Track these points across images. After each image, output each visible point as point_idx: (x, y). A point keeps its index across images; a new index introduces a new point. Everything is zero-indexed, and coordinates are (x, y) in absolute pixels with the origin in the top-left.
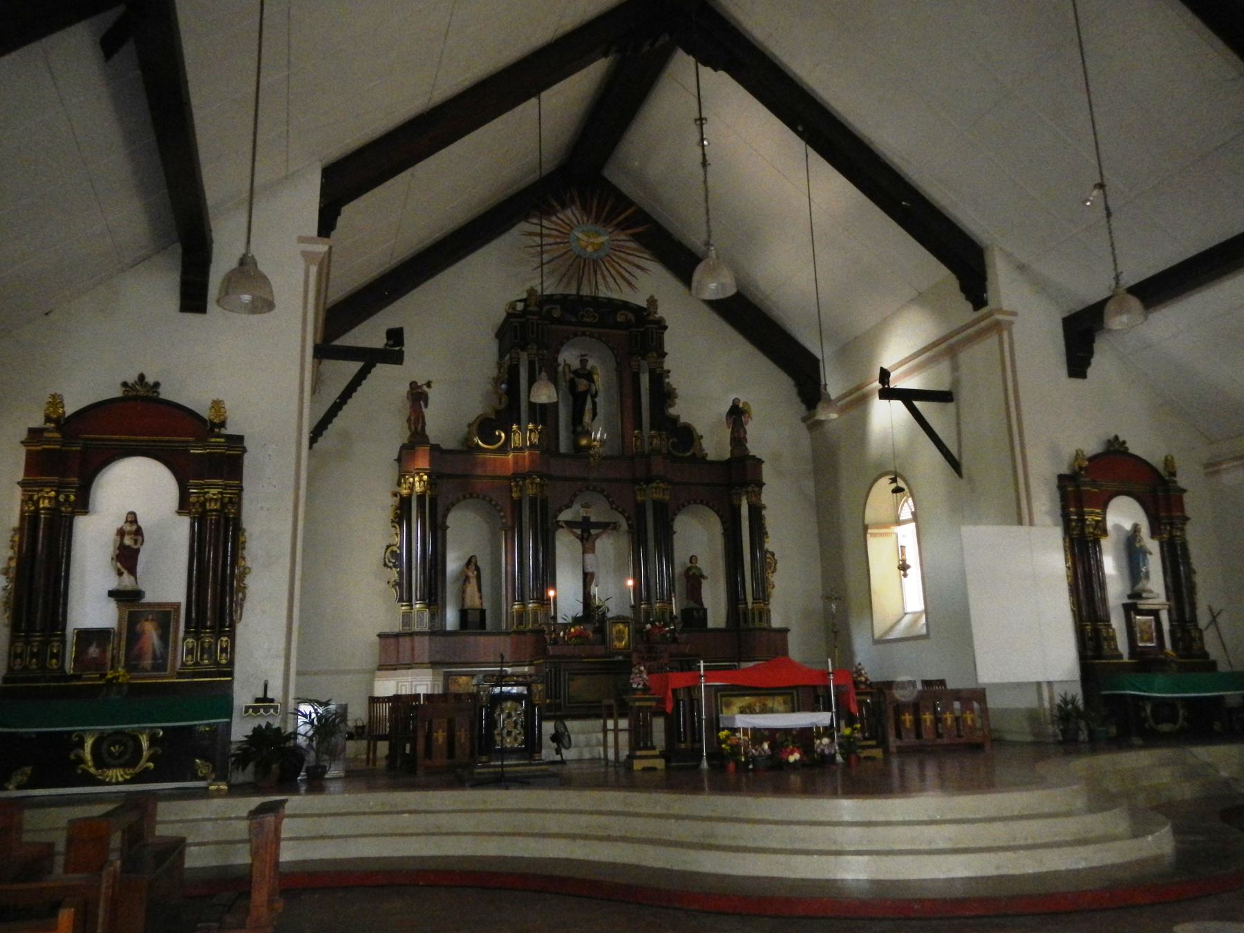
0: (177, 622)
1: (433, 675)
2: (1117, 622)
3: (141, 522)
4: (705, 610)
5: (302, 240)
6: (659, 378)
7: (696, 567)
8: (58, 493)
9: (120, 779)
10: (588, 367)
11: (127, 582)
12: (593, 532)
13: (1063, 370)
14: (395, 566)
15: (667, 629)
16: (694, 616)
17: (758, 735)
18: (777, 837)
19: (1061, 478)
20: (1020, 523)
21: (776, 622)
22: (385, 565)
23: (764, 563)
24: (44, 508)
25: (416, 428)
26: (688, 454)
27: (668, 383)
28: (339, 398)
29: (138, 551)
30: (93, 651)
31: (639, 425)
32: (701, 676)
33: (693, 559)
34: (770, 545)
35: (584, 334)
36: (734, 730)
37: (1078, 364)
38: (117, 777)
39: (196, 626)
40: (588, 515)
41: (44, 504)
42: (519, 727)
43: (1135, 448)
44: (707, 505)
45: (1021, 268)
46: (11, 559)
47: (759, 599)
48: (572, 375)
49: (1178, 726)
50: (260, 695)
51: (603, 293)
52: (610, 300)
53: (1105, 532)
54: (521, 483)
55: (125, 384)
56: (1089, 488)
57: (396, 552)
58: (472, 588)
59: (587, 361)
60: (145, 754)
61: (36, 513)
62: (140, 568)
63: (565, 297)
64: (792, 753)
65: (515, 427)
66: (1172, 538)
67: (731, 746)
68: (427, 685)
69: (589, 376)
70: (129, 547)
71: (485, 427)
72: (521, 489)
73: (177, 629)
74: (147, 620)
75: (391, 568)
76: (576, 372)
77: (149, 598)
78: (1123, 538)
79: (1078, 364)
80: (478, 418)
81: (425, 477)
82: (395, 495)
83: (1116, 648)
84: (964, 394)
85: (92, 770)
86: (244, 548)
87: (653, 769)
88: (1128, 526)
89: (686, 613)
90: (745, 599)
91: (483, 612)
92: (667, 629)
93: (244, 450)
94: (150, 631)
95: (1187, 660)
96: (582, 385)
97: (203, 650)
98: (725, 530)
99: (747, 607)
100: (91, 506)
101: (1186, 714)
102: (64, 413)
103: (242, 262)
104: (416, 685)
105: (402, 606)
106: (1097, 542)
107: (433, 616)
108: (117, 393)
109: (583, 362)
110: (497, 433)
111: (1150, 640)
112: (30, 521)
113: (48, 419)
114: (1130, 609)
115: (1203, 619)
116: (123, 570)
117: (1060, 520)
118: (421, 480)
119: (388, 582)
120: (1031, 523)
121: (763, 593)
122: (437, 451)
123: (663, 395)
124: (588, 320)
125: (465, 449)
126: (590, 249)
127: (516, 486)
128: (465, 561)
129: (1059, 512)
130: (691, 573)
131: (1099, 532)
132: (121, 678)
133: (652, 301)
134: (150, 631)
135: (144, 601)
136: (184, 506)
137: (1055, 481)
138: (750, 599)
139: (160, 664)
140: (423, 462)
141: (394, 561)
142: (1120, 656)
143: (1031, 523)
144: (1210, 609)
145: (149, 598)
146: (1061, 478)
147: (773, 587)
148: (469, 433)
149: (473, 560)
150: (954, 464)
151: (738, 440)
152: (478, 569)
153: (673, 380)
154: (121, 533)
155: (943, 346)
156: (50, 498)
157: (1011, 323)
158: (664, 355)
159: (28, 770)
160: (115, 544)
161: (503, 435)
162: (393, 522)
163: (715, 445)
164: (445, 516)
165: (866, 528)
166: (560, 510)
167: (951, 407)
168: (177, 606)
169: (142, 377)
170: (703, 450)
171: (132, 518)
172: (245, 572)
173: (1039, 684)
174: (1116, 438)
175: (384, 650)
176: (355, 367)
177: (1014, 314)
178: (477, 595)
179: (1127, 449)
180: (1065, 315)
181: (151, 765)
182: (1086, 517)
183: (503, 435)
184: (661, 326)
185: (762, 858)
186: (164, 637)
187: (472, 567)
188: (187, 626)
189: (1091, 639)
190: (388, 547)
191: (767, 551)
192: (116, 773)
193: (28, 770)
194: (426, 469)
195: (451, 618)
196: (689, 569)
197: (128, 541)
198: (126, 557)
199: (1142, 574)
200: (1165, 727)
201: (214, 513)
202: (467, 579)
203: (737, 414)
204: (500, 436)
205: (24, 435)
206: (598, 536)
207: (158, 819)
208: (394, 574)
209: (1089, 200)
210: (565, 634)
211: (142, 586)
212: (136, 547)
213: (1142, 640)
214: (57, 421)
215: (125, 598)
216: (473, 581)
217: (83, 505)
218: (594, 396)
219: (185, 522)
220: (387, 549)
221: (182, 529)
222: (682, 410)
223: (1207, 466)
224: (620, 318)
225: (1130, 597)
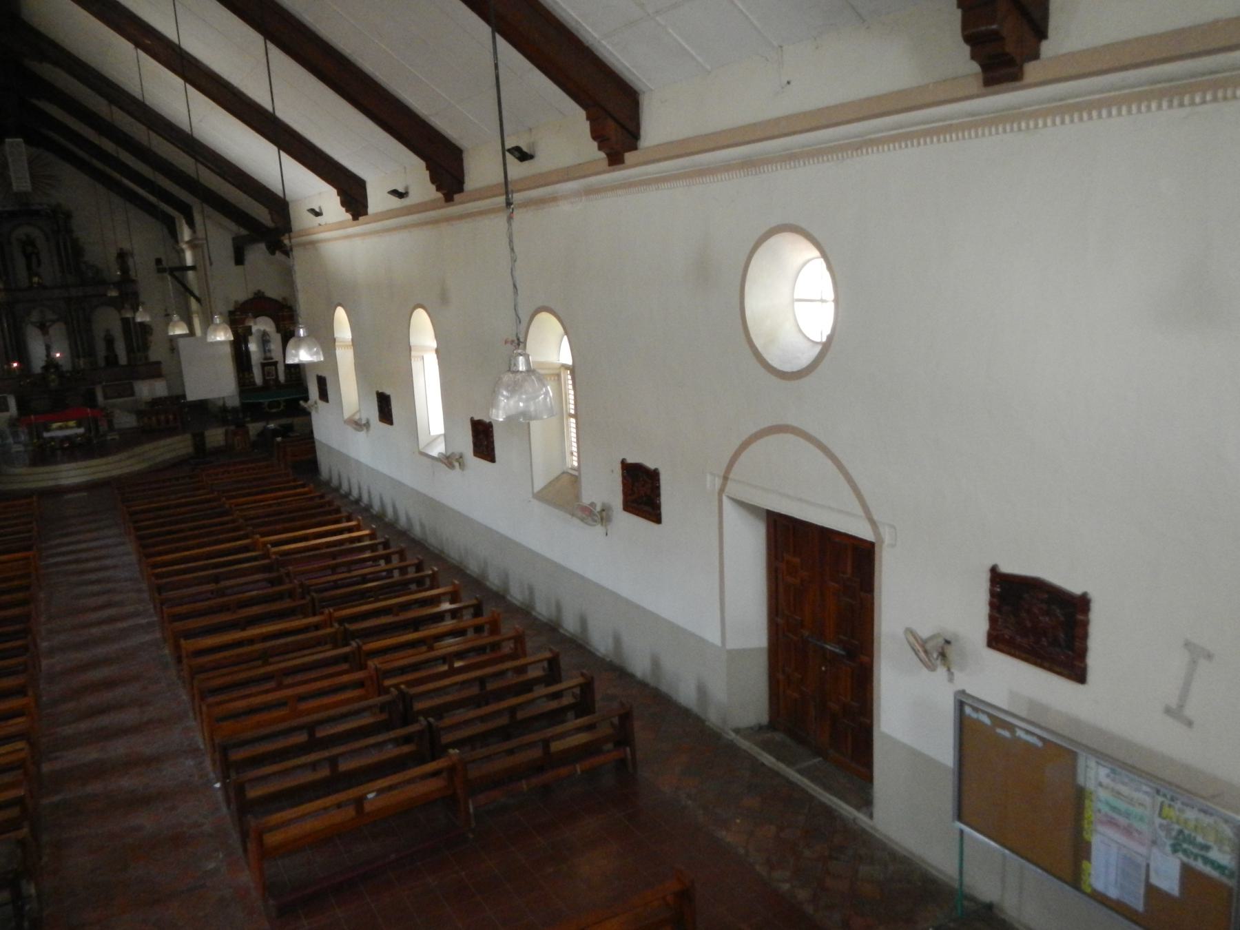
4: (116, 356)
12: (48, 324)
13: (232, 262)
16: (112, 360)
17: (52, 439)
33: (108, 331)
36: (44, 439)
37: (239, 260)
79: (239, 260)
83: (254, 381)
89: (107, 358)
114: (263, 365)
121: (145, 347)
123: (77, 250)
142: (254, 383)
151: (125, 270)
184: (68, 216)
200: (274, 410)
203: (122, 256)
206: (50, 326)
213: (268, 376)
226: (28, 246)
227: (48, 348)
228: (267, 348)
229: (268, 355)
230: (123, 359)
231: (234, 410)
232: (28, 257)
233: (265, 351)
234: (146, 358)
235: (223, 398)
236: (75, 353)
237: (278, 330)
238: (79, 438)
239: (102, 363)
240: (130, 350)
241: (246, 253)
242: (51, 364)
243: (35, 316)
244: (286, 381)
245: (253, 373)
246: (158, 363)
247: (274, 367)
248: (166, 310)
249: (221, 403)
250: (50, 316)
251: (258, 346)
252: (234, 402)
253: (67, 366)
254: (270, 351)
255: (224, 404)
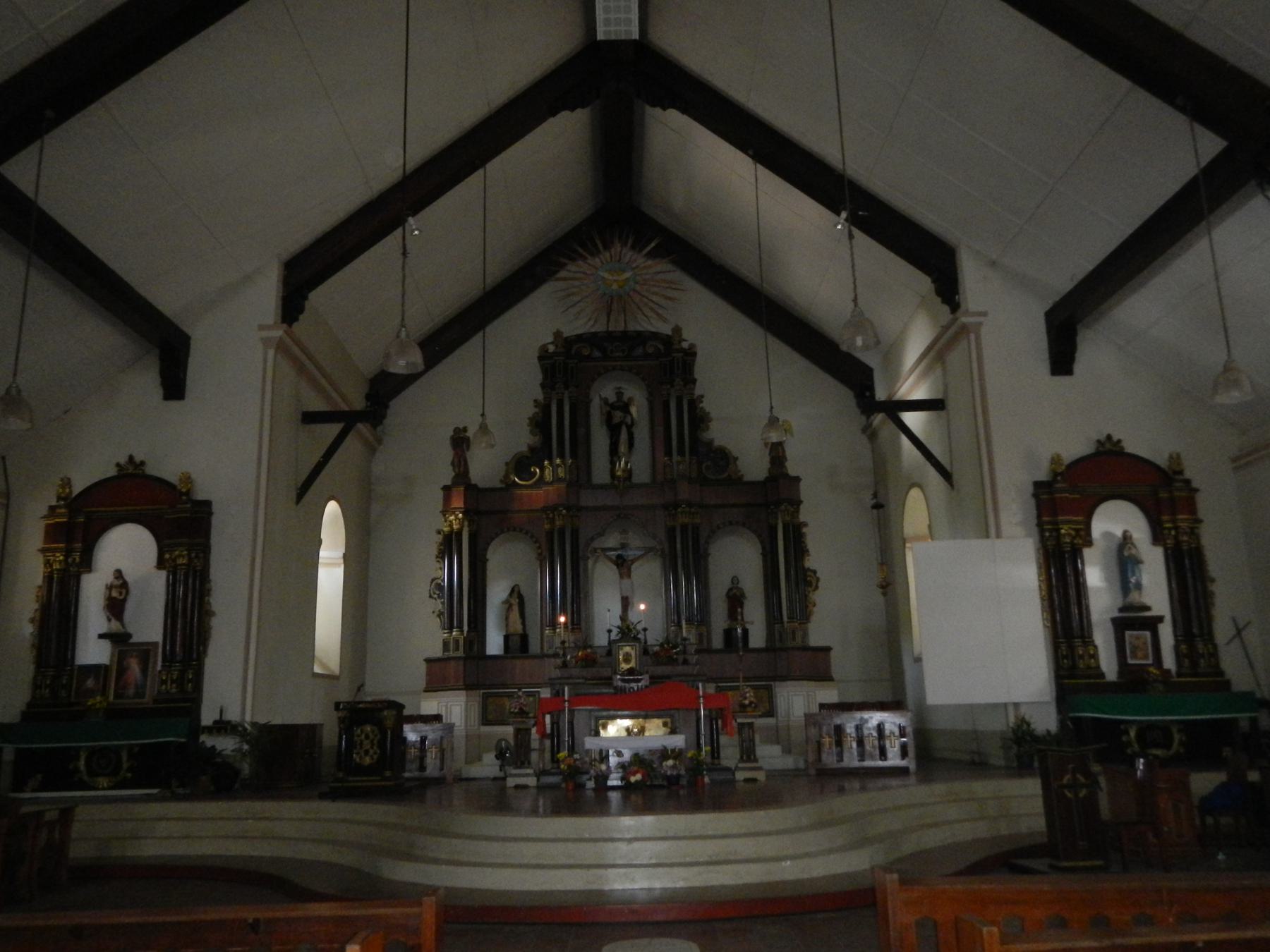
0: (156, 654)
1: (467, 696)
2: (1103, 639)
3: (128, 578)
5: (262, 328)
6: (694, 404)
7: (737, 588)
8: (67, 557)
9: (105, 785)
10: (625, 398)
11: (115, 626)
13: (1045, 367)
14: (439, 597)
15: (674, 651)
18: (528, 852)
19: (1038, 485)
20: (987, 536)
21: (815, 640)
22: (431, 597)
23: (804, 580)
24: (57, 570)
25: (459, 471)
26: (725, 475)
27: (702, 408)
28: (322, 457)
29: (124, 600)
30: (90, 683)
31: (669, 453)
32: (565, 701)
33: (735, 580)
34: (810, 563)
35: (614, 368)
36: (588, 752)
37: (1062, 361)
38: (103, 784)
39: (169, 659)
40: (625, 542)
41: (56, 566)
42: (375, 748)
43: (1133, 446)
44: (744, 525)
45: (993, 264)
46: (36, 610)
47: (793, 618)
48: (608, 409)
49: (1172, 752)
50: (217, 717)
51: (633, 327)
52: (639, 333)
53: (1089, 543)
54: (551, 515)
55: (118, 465)
56: (1067, 495)
57: (440, 584)
58: (515, 615)
59: (622, 393)
60: (125, 766)
61: (51, 573)
62: (128, 615)
63: (595, 334)
64: (634, 774)
65: (546, 462)
66: (1178, 543)
67: (569, 766)
68: (461, 706)
69: (625, 408)
70: (115, 598)
71: (521, 465)
72: (552, 521)
73: (155, 663)
74: (132, 657)
75: (435, 599)
76: (613, 407)
77: (134, 639)
78: (1114, 547)
79: (1062, 361)
80: (514, 457)
81: (460, 515)
82: (439, 532)
83: (1098, 667)
84: (950, 404)
85: (86, 778)
86: (209, 595)
87: (525, 787)
88: (1119, 533)
89: (729, 634)
90: (782, 618)
91: (524, 638)
92: (674, 651)
93: (210, 514)
94: (134, 666)
95: (1194, 679)
96: (618, 416)
97: (173, 682)
98: (764, 548)
99: (783, 626)
100: (93, 568)
101: (1184, 738)
102: (71, 492)
103: (8, 391)
104: (451, 705)
105: (445, 633)
106: (1076, 553)
107: (469, 643)
108: (112, 472)
109: (619, 394)
110: (532, 470)
111: (1146, 657)
112: (49, 578)
113: (59, 498)
115: (1222, 630)
116: (111, 617)
117: (1035, 530)
118: (457, 518)
119: (433, 612)
120: (998, 536)
121: (803, 612)
122: (472, 491)
123: (699, 420)
124: (617, 354)
125: (503, 486)
126: (615, 287)
127: (547, 518)
128: (509, 592)
129: (1035, 521)
130: (731, 594)
131: (1080, 542)
132: (98, 704)
133: (677, 330)
134: (134, 666)
135: (132, 641)
136: (161, 564)
137: (1030, 489)
138: (785, 619)
139: (140, 694)
140: (458, 502)
141: (438, 592)
142: (1102, 675)
143: (998, 536)
144: (1234, 620)
145: (134, 639)
146: (1038, 485)
147: (814, 605)
148: (507, 471)
149: (516, 589)
150: (946, 474)
152: (521, 598)
153: (706, 405)
154: (110, 588)
155: (932, 354)
156: (60, 561)
157: (980, 324)
158: (694, 381)
159: (39, 777)
160: (105, 596)
161: (538, 470)
162: (437, 557)
163: (754, 466)
164: (486, 550)
165: (904, 541)
166: (592, 539)
167: (943, 413)
168: (155, 644)
169: (131, 458)
170: (739, 471)
171: (119, 574)
172: (210, 614)
173: (1005, 705)
174: (1109, 437)
175: (429, 673)
176: (334, 429)
177: (984, 314)
178: (519, 621)
179: (1122, 448)
180: (1047, 308)
181: (129, 775)
182: (1061, 526)
183: (538, 470)
184: (691, 353)
185: (507, 872)
186: (144, 671)
187: (515, 595)
188: (164, 660)
189: (1065, 657)
190: (433, 580)
191: (809, 569)
192: (103, 781)
193: (39, 777)
194: (461, 508)
195: (494, 643)
196: (730, 590)
197: (114, 594)
198: (115, 607)
199: (1131, 585)
201: (183, 567)
202: (511, 606)
204: (535, 473)
205: (45, 512)
206: (633, 561)
207: (76, 818)
208: (439, 605)
209: (839, 223)
210: (571, 658)
211: (130, 630)
212: (121, 597)
213: (1134, 656)
214: (64, 499)
215: (118, 639)
216: (516, 608)
217: (87, 564)
218: (630, 428)
219: (163, 574)
220: (432, 582)
221: (159, 581)
222: (718, 434)
223: (1234, 460)
224: (650, 350)
225: (1121, 610)
226: (617, 408)
227: (626, 603)
228: (1133, 580)
229: (1134, 597)
230: (757, 638)
231: (1048, 738)
232: (614, 430)
233: (1125, 588)
234: (805, 635)
235: (1016, 705)
236: (674, 615)
237: (1157, 539)
238: (670, 762)
239: (717, 642)
240: (773, 617)
241: (1079, 339)
242: (627, 632)
243: (612, 540)
244: (1179, 675)
245: (1092, 643)
246: (827, 650)
247: (1148, 634)
248: (875, 495)
249: (997, 724)
250: (636, 542)
251: (1106, 569)
252: (1046, 721)
253: (655, 637)
254: (1139, 586)
255: (1023, 722)
